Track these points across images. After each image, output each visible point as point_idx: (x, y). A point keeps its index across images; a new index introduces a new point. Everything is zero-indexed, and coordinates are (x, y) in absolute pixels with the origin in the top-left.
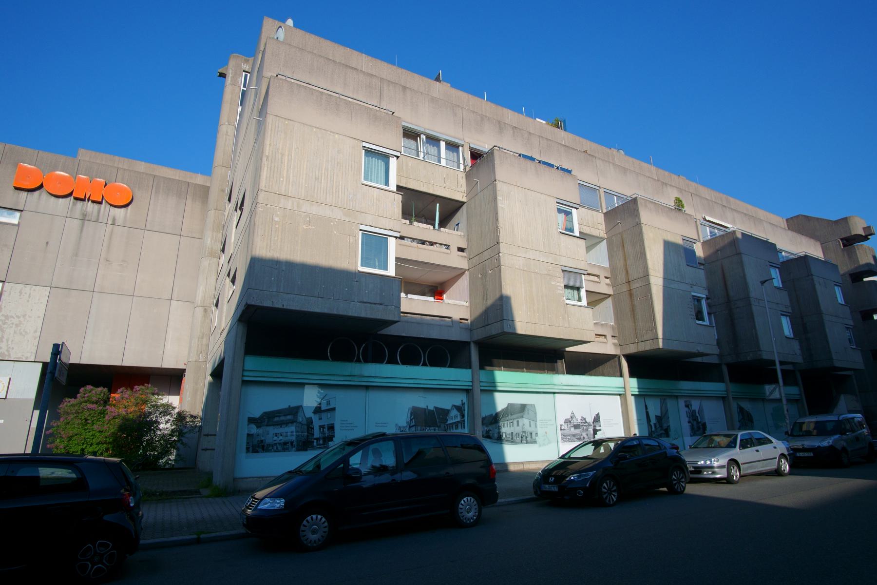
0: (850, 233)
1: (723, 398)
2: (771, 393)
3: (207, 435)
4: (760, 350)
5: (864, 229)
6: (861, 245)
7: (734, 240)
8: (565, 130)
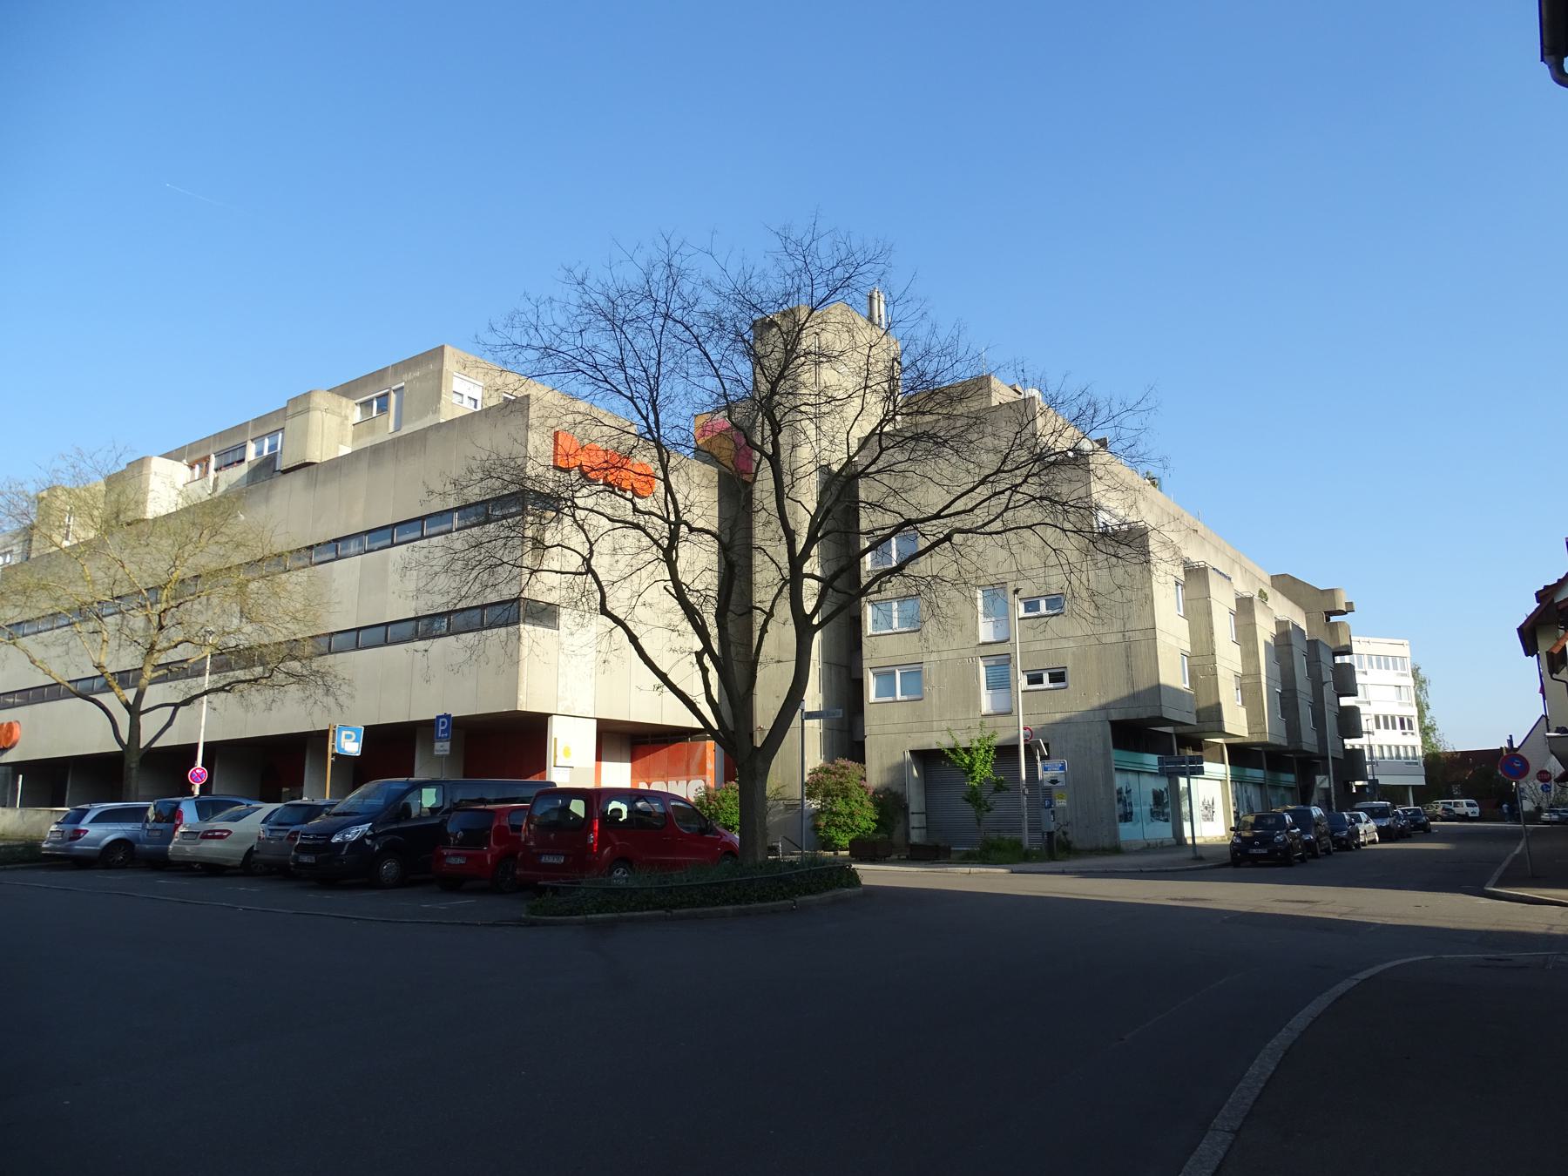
1: (1261, 785)
2: (1321, 783)
3: (913, 813)
6: (1344, 622)
7: (1287, 632)
8: (1160, 490)
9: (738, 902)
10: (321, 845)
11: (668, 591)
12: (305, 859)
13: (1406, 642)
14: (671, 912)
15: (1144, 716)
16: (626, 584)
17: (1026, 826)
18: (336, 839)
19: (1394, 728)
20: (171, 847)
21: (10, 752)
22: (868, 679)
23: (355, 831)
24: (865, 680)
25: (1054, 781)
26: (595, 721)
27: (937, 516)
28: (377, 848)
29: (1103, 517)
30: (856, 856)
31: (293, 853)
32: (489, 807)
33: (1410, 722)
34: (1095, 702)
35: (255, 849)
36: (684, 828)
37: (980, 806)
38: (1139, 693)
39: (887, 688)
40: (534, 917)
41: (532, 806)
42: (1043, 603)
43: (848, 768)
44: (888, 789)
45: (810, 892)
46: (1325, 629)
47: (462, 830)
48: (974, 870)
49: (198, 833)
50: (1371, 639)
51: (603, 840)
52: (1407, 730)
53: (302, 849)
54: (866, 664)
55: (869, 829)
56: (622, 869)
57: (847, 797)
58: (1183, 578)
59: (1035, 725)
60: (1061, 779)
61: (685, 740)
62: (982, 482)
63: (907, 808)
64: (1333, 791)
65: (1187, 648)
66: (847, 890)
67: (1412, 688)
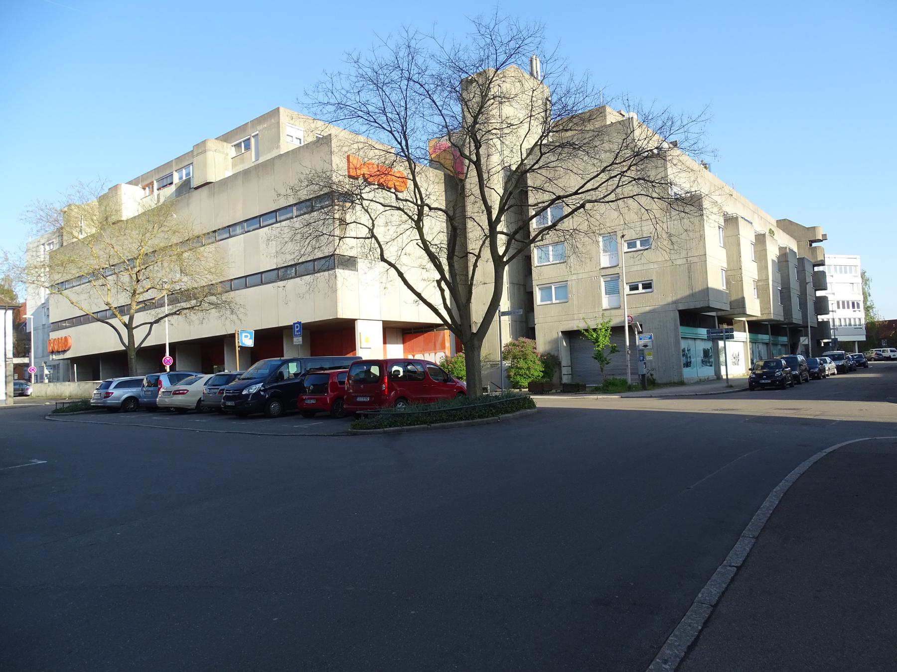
0: (815, 238)
1: (767, 344)
2: (803, 341)
3: (564, 366)
4: (792, 318)
5: (822, 235)
7: (785, 253)
8: (710, 171)
9: (467, 419)
10: (237, 396)
11: (419, 245)
12: (229, 403)
13: (858, 257)
14: (431, 426)
15: (699, 307)
16: (395, 243)
17: (629, 372)
18: (244, 392)
19: (848, 307)
20: (157, 399)
21: (68, 352)
22: (536, 292)
23: (254, 388)
24: (534, 293)
25: (646, 346)
26: (381, 322)
27: (576, 193)
28: (267, 396)
29: (675, 189)
30: (532, 391)
31: (222, 401)
32: (326, 372)
33: (858, 304)
34: (670, 299)
35: (202, 399)
36: (435, 379)
37: (602, 361)
38: (696, 293)
39: (547, 295)
40: (355, 430)
41: (350, 370)
42: (638, 243)
43: (526, 343)
44: (549, 354)
45: (507, 412)
46: (809, 251)
47: (313, 385)
48: (599, 397)
49: (171, 392)
50: (836, 256)
51: (390, 388)
52: (856, 309)
53: (227, 398)
54: (534, 283)
55: (539, 376)
56: (402, 403)
57: (526, 359)
58: (723, 224)
59: (634, 313)
60: (650, 344)
61: (433, 330)
62: (603, 171)
63: (560, 364)
64: (810, 346)
65: (725, 265)
66: (529, 410)
67: (861, 284)
